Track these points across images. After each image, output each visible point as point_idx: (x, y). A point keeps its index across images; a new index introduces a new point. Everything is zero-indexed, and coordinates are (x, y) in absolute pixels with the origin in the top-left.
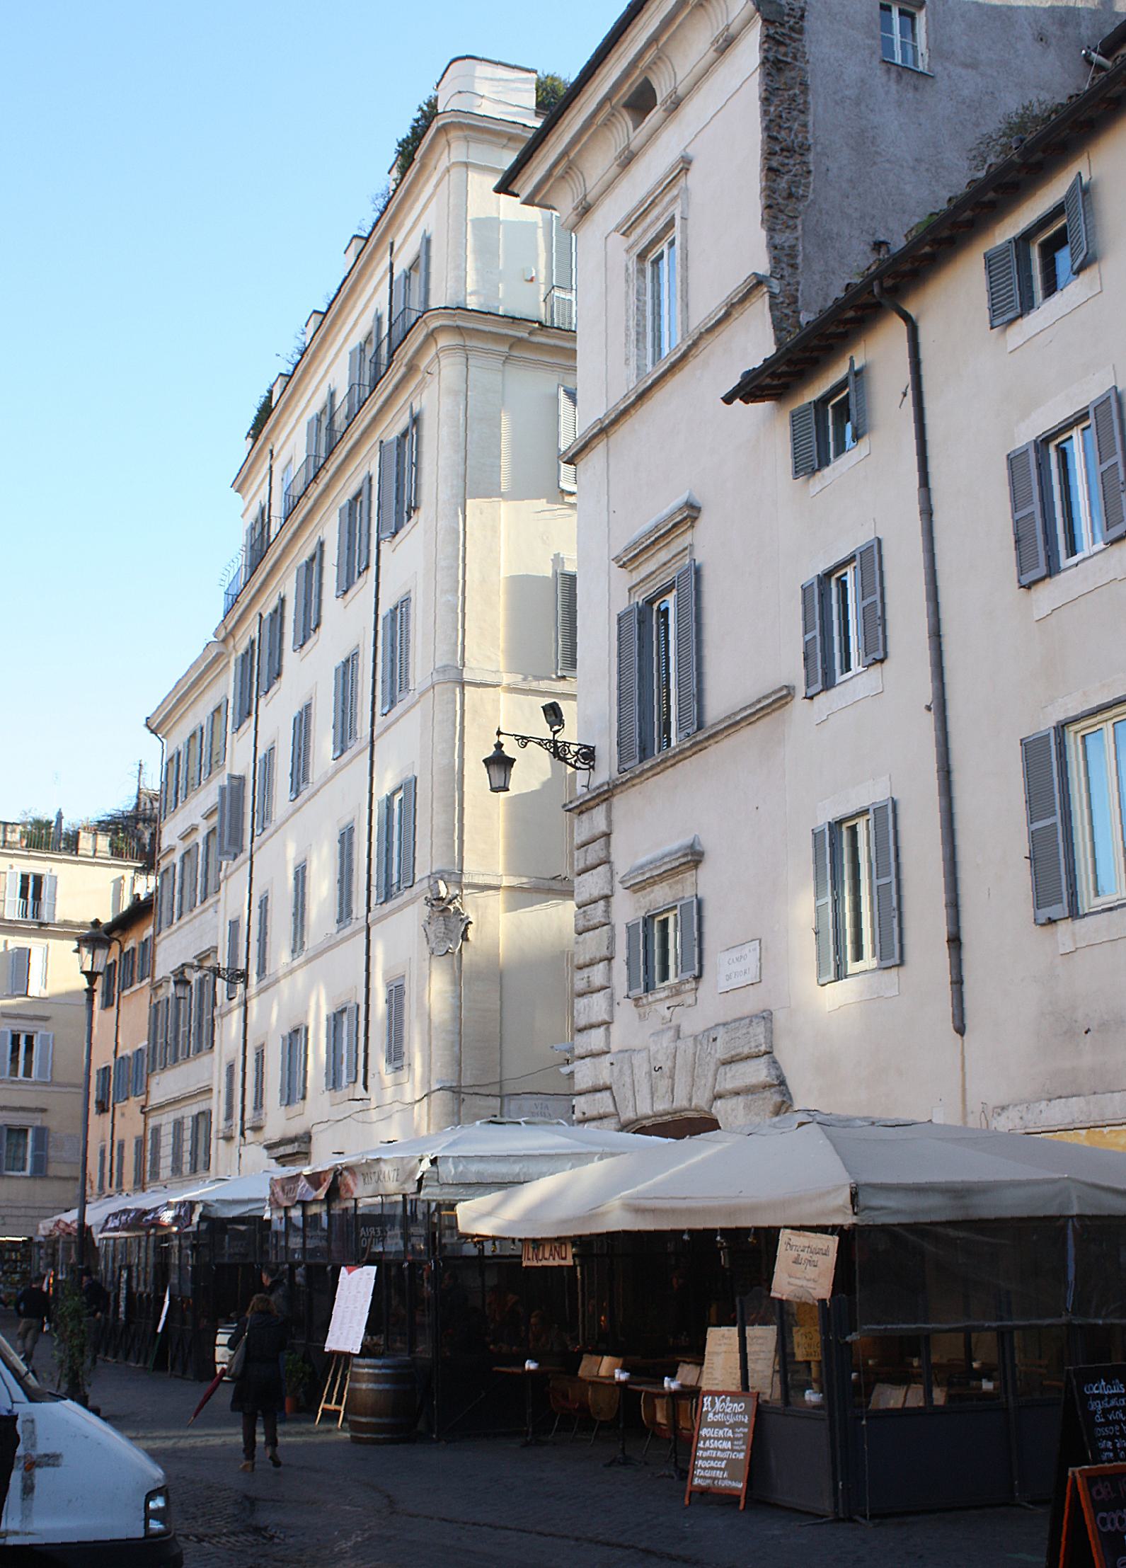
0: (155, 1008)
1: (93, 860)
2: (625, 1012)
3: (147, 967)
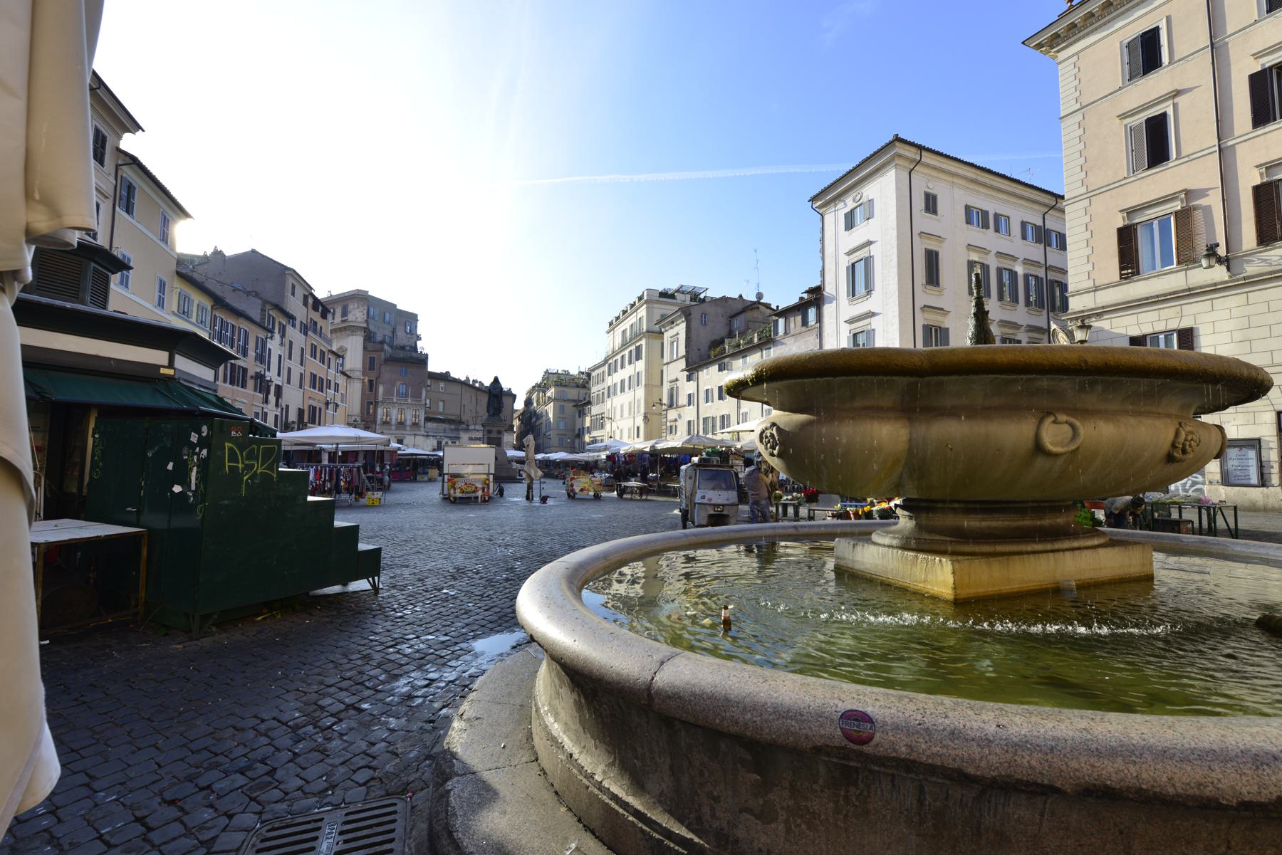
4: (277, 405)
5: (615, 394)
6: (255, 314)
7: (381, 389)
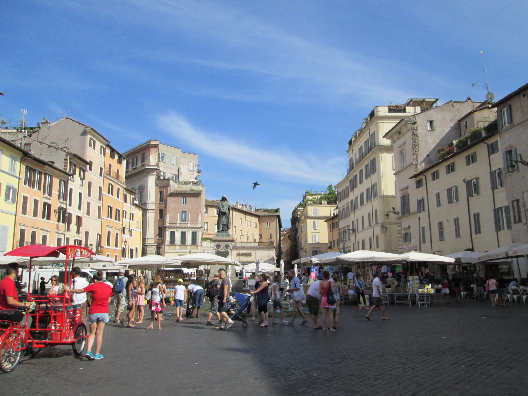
0: (340, 233)
1: (325, 206)
2: (404, 244)
3: (338, 226)
4: (78, 232)
5: (357, 207)
6: (59, 164)
7: (168, 217)
